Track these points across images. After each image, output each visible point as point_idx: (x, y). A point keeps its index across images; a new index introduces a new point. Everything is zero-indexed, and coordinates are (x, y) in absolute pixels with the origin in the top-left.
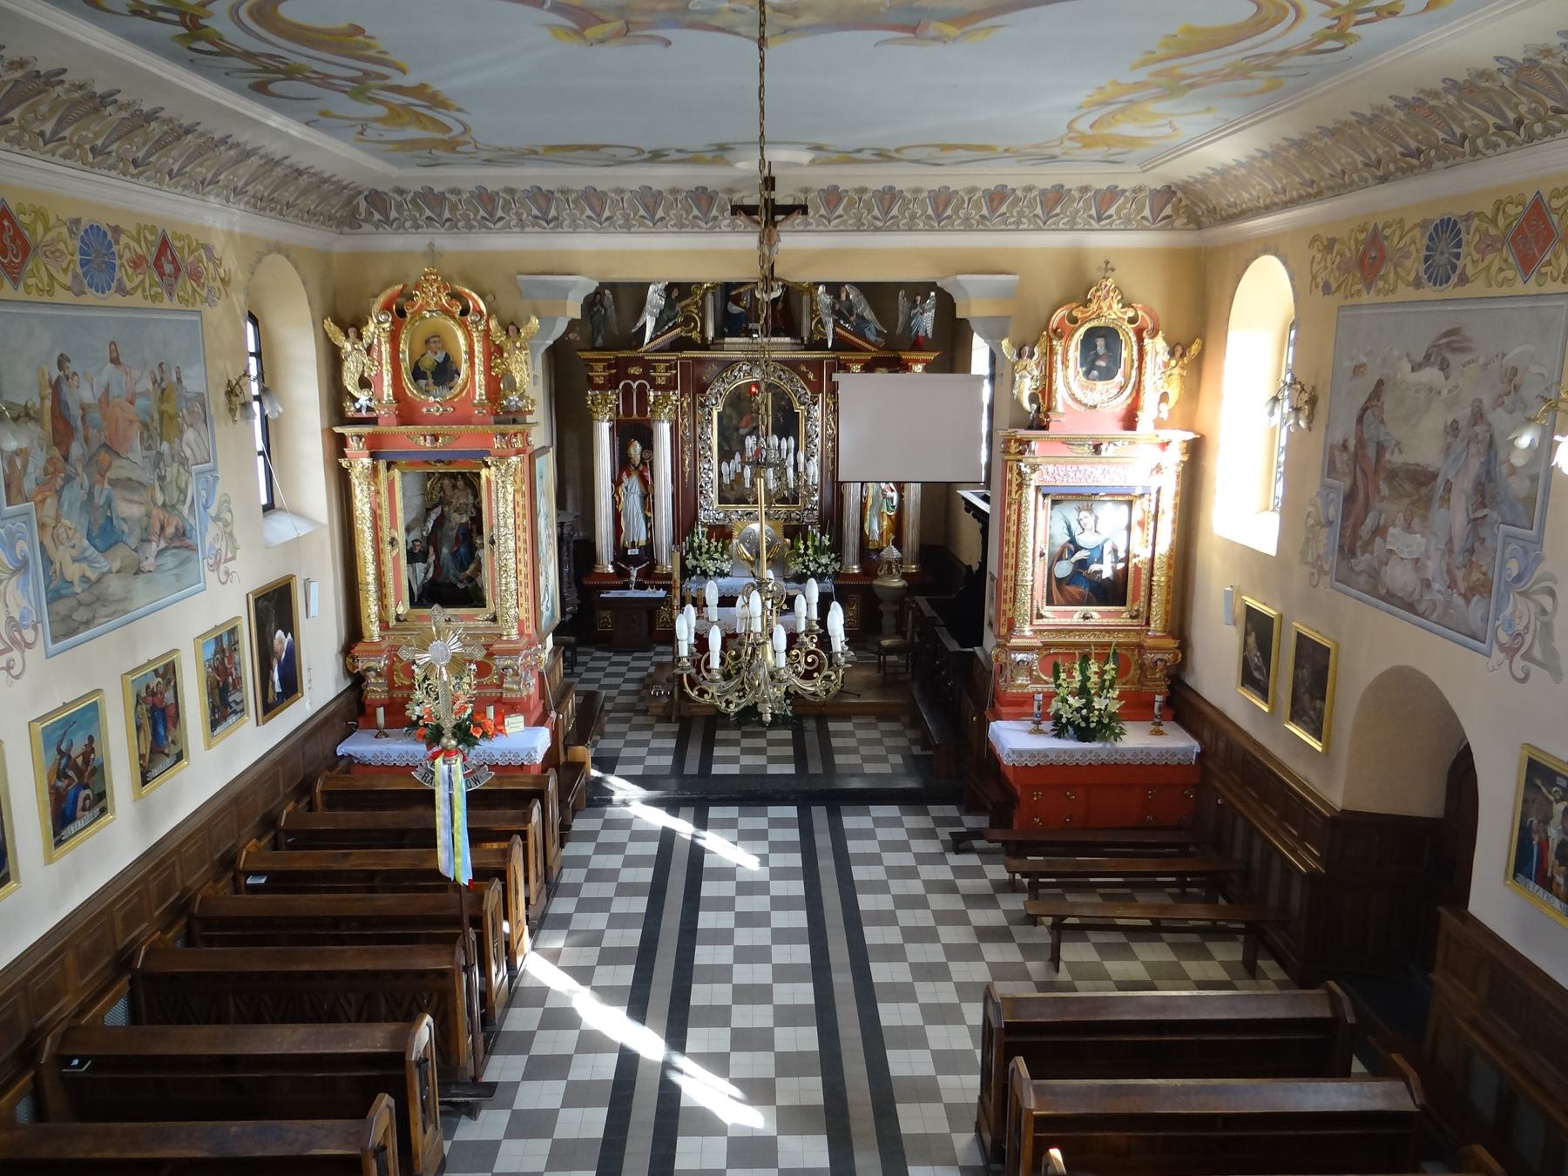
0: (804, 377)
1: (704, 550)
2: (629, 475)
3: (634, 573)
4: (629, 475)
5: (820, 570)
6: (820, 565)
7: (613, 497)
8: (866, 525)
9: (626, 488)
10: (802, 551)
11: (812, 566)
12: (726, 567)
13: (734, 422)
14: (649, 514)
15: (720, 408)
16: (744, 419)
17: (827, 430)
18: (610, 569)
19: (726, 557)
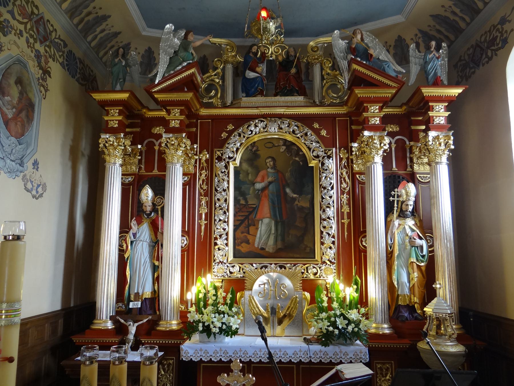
0: (317, 132)
1: (210, 302)
2: (139, 223)
3: (133, 329)
4: (139, 223)
5: (350, 328)
6: (350, 322)
7: (120, 246)
8: (394, 277)
9: (134, 235)
10: (325, 304)
11: (340, 323)
12: (234, 323)
13: (250, 177)
14: (157, 263)
15: (238, 162)
16: (261, 173)
17: (341, 183)
18: (110, 325)
19: (234, 309)
